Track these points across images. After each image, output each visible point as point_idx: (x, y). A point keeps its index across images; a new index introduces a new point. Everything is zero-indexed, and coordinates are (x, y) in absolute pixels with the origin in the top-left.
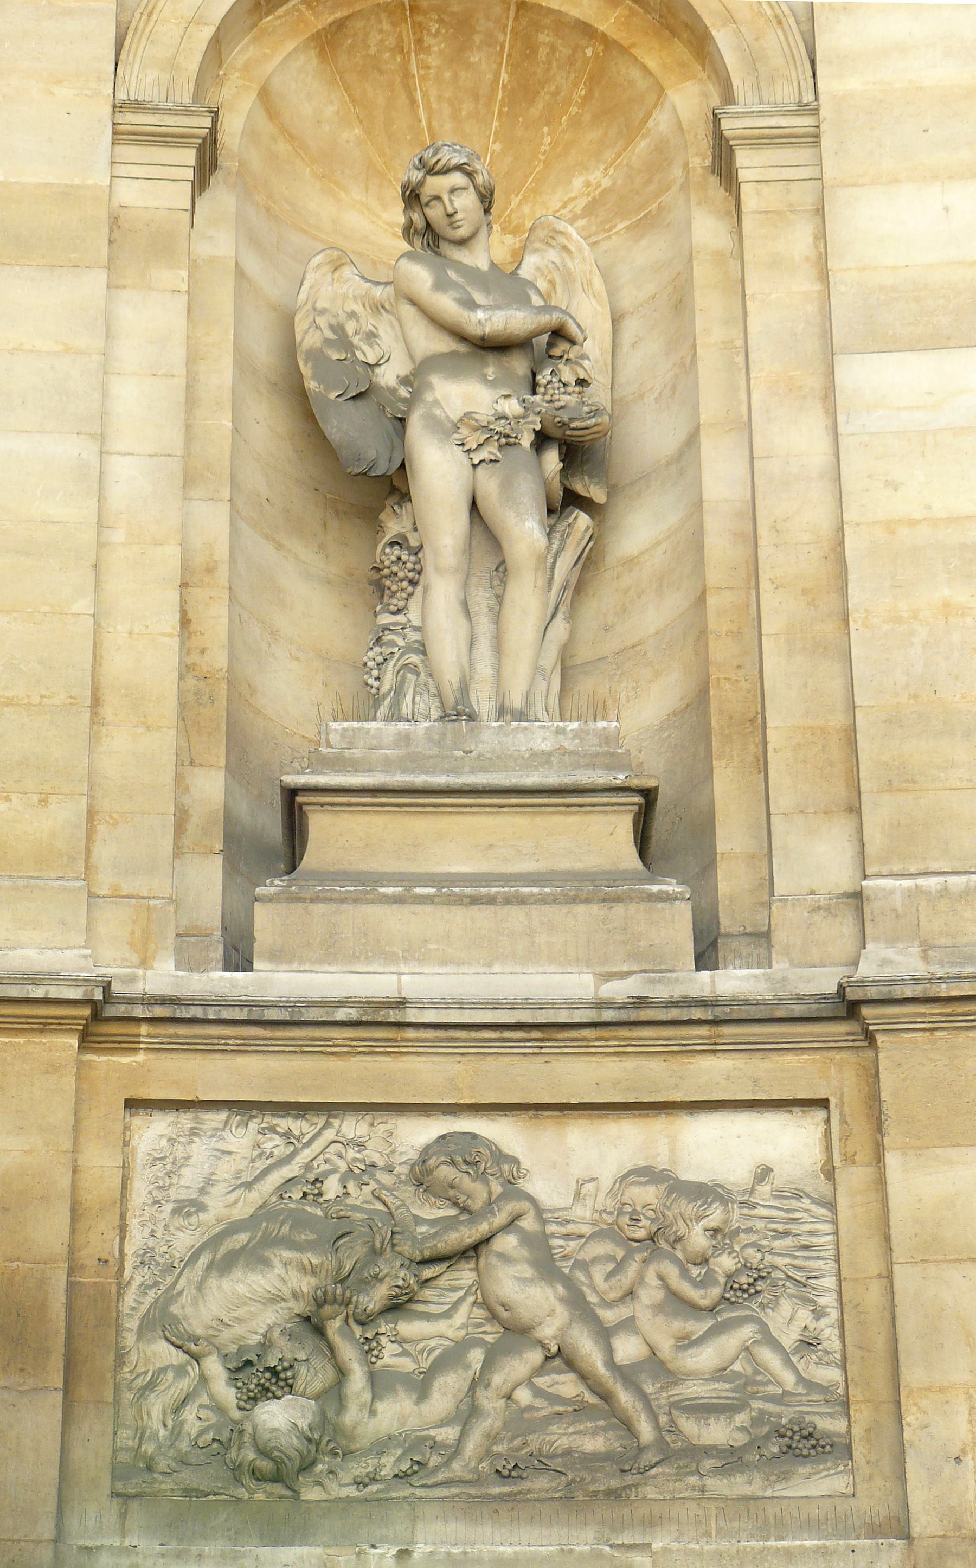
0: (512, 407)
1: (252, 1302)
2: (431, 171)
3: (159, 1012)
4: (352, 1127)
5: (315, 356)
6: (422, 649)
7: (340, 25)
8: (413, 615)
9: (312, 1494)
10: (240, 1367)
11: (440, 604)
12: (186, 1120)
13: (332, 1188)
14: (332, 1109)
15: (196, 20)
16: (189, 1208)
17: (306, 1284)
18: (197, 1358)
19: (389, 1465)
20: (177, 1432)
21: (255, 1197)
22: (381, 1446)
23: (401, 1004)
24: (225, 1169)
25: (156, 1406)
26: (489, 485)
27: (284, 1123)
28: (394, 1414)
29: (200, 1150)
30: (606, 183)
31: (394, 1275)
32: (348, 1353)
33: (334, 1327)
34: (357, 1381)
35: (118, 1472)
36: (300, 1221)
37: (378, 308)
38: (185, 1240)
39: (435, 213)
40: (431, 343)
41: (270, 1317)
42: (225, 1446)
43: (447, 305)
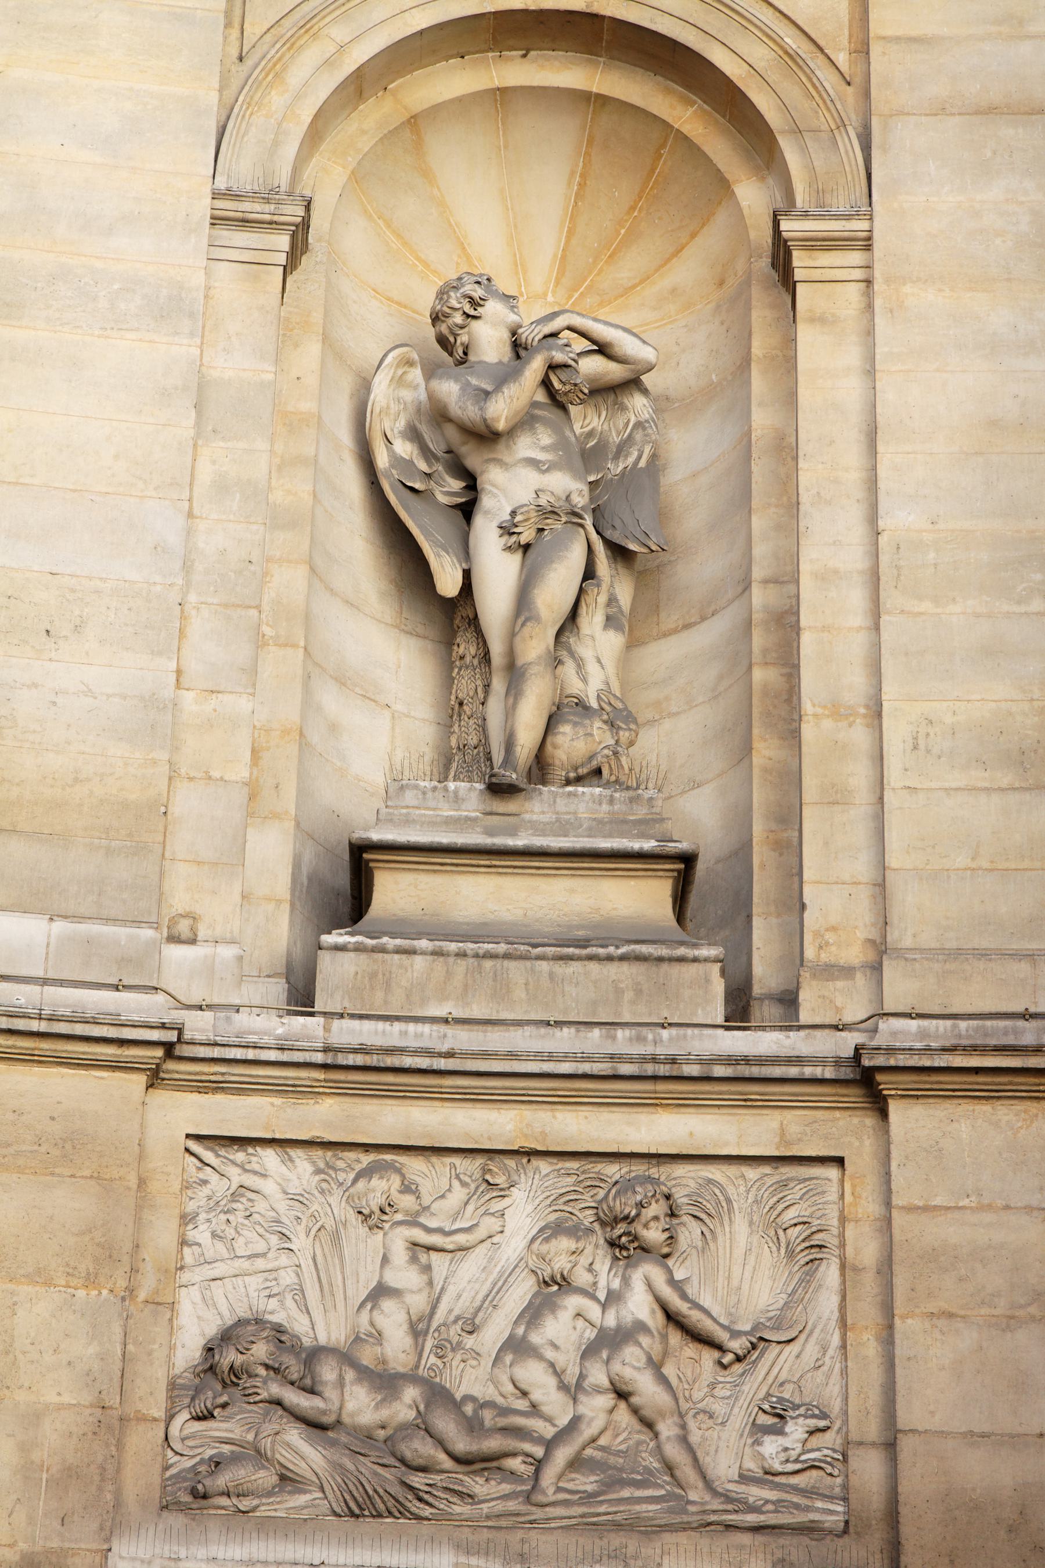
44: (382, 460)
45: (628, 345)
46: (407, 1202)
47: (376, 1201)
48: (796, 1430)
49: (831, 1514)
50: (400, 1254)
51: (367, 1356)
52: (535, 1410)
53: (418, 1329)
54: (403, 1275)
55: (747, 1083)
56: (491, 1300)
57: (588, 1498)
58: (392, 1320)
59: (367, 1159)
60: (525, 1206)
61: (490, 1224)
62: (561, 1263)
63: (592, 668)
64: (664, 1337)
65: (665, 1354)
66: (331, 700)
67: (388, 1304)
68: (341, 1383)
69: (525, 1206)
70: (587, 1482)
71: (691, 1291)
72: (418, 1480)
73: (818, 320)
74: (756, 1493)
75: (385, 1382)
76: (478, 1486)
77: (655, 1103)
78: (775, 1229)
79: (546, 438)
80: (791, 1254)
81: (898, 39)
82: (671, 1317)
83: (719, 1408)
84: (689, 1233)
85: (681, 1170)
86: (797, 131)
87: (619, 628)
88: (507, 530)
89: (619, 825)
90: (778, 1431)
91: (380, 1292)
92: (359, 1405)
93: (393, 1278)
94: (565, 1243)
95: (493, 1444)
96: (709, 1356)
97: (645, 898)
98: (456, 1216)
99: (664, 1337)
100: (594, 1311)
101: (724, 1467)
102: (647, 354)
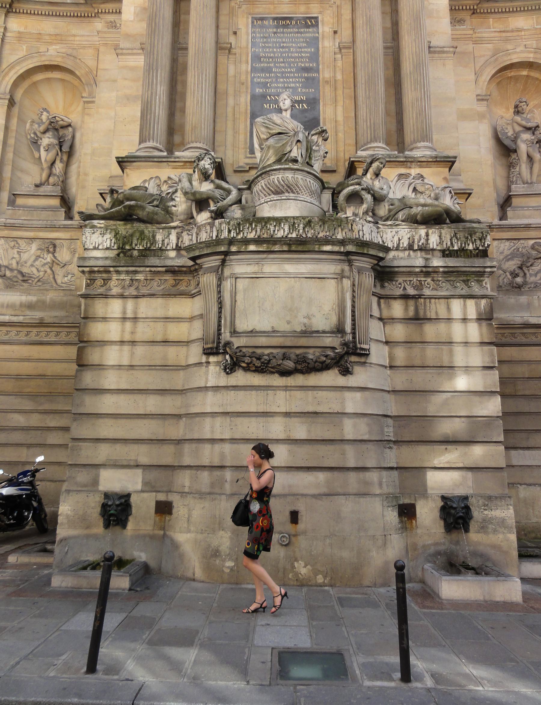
0: (533, 138)
1: (512, 265)
2: (521, 102)
3: (497, 227)
4: (522, 241)
5: (500, 132)
6: (519, 174)
7: (500, 81)
8: (517, 169)
9: (522, 290)
10: (511, 273)
11: (524, 167)
12: (500, 241)
13: (520, 250)
14: (519, 239)
15: (485, 81)
16: (502, 253)
17: (519, 263)
18: (505, 273)
19: (532, 286)
20: (504, 282)
21: (510, 251)
22: (531, 283)
23: (531, 224)
24: (506, 248)
25: (501, 279)
26: (530, 150)
27: (513, 241)
28: (533, 279)
29: (502, 245)
30: (537, 103)
31: (532, 261)
32: (526, 271)
33: (524, 268)
34: (528, 275)
35: (498, 288)
36: (518, 254)
37: (508, 124)
38: (502, 257)
39: (520, 109)
40: (518, 128)
41: (514, 267)
42: (510, 284)
43: (524, 123)
44: (29, 137)
45: (66, 119)
46: (17, 245)
47: (12, 245)
48: (70, 276)
49: (73, 288)
50: (16, 253)
51: (10, 267)
52: (34, 274)
53: (17, 263)
54: (16, 256)
55: (66, 227)
56: (29, 259)
57: (40, 286)
58: (14, 262)
59: (12, 239)
60: (34, 247)
61: (29, 248)
62: (39, 254)
63: (57, 169)
64: (53, 264)
65: (53, 266)
66: (19, 174)
67: (14, 260)
68: (5, 270)
69: (34, 247)
70: (39, 284)
71: (57, 258)
72: (15, 283)
73: (88, 114)
74: (63, 285)
75: (12, 270)
76: (24, 284)
77: (53, 231)
78: (69, 248)
79: (51, 133)
80: (71, 252)
81: (102, 69)
82: (53, 261)
83: (59, 273)
84: (58, 250)
85: (57, 241)
86: (87, 85)
87: (63, 163)
88: (44, 148)
89: (53, 191)
90: (67, 277)
91: (13, 258)
92: (8, 273)
93: (15, 256)
94: (40, 251)
95: (25, 279)
96: (59, 266)
97: (56, 202)
98: (25, 247)
99: (53, 264)
100: (43, 260)
101: (59, 281)
102: (70, 121)
